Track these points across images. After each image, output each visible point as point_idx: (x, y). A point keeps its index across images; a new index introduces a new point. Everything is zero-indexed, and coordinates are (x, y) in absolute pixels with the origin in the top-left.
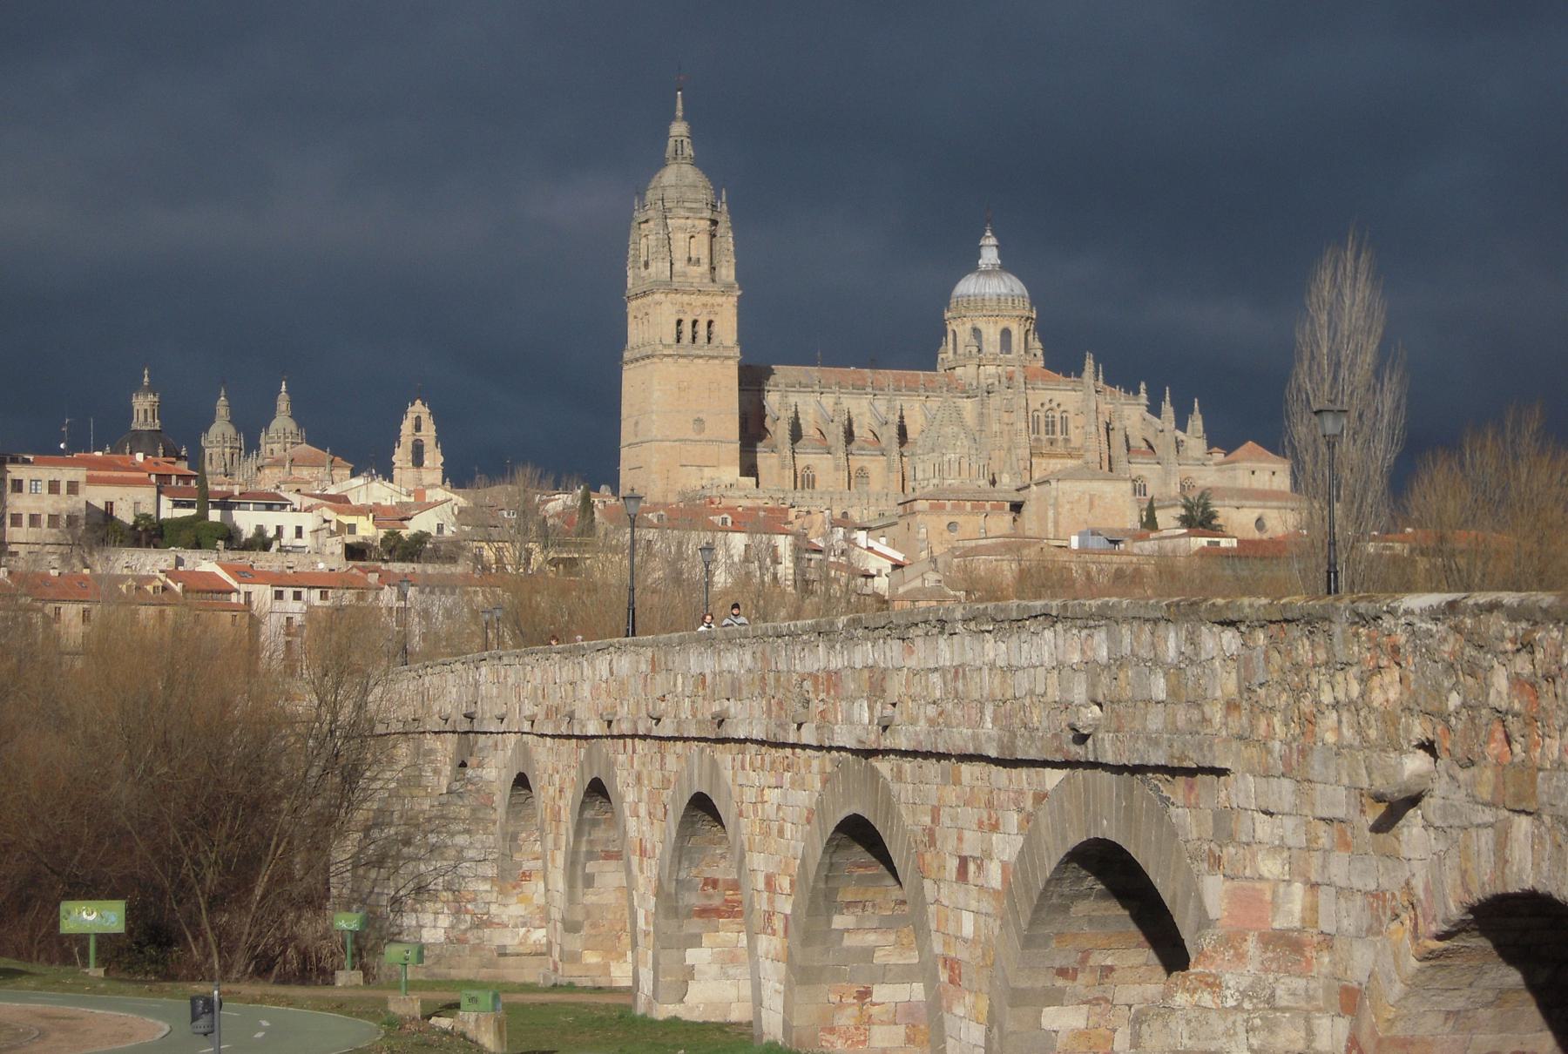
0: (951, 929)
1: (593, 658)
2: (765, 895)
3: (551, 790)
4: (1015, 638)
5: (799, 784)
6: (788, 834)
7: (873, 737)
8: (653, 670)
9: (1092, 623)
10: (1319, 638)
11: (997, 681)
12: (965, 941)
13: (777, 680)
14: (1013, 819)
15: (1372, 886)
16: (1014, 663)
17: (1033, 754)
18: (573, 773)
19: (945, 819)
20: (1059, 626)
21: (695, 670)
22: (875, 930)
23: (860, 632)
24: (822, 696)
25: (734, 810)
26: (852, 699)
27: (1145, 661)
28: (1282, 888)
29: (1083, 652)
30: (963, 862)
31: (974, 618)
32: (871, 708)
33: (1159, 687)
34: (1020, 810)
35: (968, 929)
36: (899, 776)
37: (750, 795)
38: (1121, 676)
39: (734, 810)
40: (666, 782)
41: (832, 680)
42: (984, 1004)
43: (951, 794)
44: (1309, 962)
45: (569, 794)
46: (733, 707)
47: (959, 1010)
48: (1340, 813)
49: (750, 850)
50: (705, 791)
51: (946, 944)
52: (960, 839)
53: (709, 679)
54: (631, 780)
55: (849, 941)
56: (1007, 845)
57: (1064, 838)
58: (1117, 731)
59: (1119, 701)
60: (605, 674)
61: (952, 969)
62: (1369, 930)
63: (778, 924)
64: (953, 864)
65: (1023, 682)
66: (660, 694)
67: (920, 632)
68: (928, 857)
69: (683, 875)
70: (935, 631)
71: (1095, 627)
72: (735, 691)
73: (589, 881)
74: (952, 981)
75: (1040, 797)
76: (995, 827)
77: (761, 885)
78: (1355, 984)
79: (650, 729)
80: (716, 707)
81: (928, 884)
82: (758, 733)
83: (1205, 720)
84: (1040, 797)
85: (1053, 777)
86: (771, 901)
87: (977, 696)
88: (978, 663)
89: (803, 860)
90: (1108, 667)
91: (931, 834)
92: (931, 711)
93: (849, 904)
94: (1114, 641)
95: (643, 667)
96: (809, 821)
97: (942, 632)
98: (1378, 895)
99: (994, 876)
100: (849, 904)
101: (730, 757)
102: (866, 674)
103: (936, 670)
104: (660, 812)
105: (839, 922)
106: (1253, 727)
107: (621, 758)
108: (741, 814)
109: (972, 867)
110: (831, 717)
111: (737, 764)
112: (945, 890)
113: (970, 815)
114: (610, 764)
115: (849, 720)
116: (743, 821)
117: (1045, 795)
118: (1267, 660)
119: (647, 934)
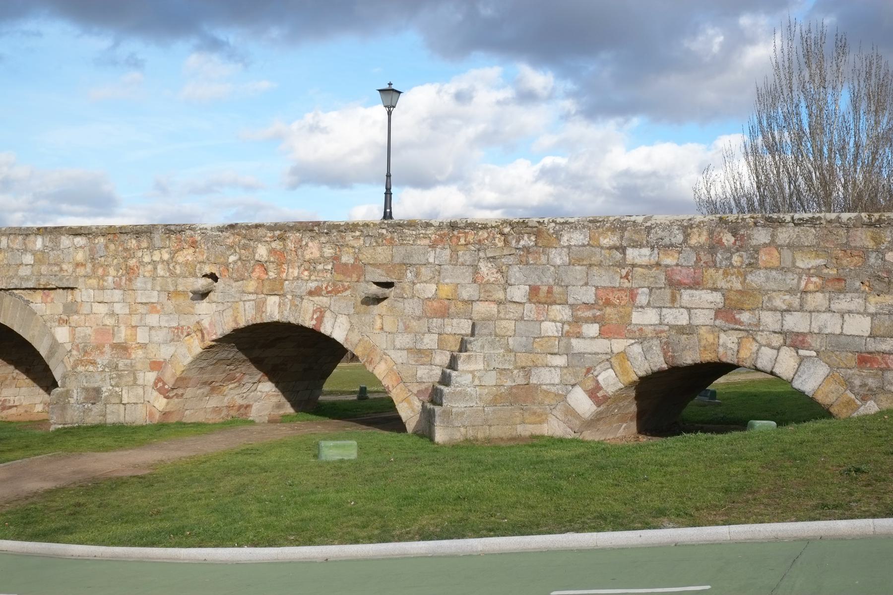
15: (175, 325)
27: (18, 250)
28: (116, 329)
33: (28, 259)
44: (130, 354)
62: (172, 340)
78: (162, 360)
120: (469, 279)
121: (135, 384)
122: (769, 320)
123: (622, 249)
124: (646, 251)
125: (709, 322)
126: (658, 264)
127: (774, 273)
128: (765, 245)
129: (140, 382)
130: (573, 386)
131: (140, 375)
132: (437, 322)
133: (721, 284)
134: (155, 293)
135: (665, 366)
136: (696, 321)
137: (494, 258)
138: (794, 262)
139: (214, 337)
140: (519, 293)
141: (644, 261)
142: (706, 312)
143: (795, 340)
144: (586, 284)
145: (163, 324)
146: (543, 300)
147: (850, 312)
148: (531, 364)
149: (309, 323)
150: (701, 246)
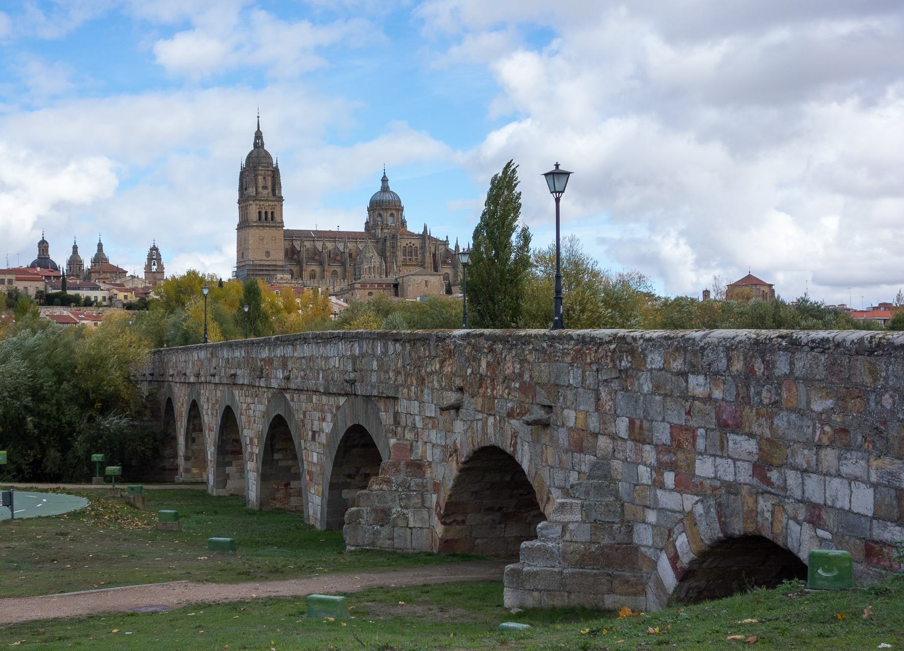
0: (310, 459)
1: (192, 352)
3: (179, 404)
4: (328, 347)
5: (260, 403)
6: (256, 422)
7: (283, 384)
8: (212, 357)
9: (353, 340)
11: (323, 363)
12: (315, 464)
13: (253, 361)
14: (329, 417)
16: (329, 355)
17: (335, 391)
18: (186, 397)
19: (307, 416)
21: (226, 356)
22: (291, 459)
23: (279, 343)
24: (267, 367)
25: (239, 412)
26: (277, 369)
29: (351, 351)
30: (314, 433)
31: (316, 337)
32: (283, 373)
34: (332, 413)
35: (315, 460)
36: (293, 400)
37: (244, 406)
38: (363, 360)
39: (239, 412)
40: (217, 401)
41: (269, 361)
42: (320, 489)
43: (310, 406)
45: (185, 405)
46: (239, 372)
51: (308, 465)
52: (312, 424)
53: (230, 361)
54: (205, 400)
55: (281, 464)
56: (327, 427)
57: (346, 423)
58: (362, 382)
59: (362, 370)
60: (196, 358)
61: (310, 476)
64: (310, 433)
66: (214, 366)
67: (298, 343)
69: (224, 438)
70: (303, 342)
71: (354, 341)
72: (239, 366)
75: (338, 408)
76: (324, 420)
77: (248, 442)
79: (211, 380)
80: (233, 372)
81: (302, 441)
82: (246, 382)
84: (338, 408)
85: (342, 400)
86: (252, 448)
87: (317, 368)
88: (317, 355)
89: (262, 431)
90: (359, 357)
91: (303, 421)
93: (280, 450)
94: (361, 347)
95: (209, 356)
96: (264, 417)
97: (305, 343)
99: (323, 439)
100: (280, 450)
102: (281, 360)
103: (304, 357)
105: (277, 456)
107: (202, 391)
108: (241, 414)
109: (317, 436)
110: (270, 376)
111: (240, 394)
112: (308, 444)
113: (317, 415)
114: (199, 394)
115: (276, 378)
117: (340, 407)
119: (211, 462)
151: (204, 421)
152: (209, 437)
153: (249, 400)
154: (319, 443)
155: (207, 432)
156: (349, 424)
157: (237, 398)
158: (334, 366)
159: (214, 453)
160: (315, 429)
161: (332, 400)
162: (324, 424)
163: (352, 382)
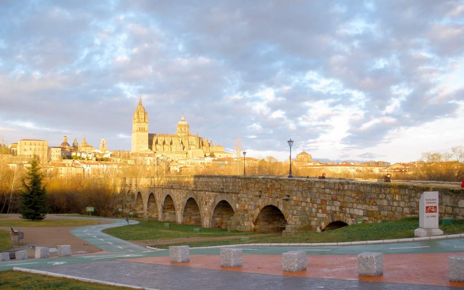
2: (178, 206)
4: (213, 179)
10: (250, 180)
16: (213, 181)
17: (216, 191)
20: (219, 178)
21: (168, 180)
25: (173, 197)
32: (194, 185)
33: (231, 184)
34: (213, 197)
36: (197, 193)
37: (176, 195)
42: (209, 218)
44: (248, 212)
45: (147, 194)
47: (205, 219)
48: (252, 198)
49: (176, 201)
50: (169, 194)
56: (212, 201)
63: (180, 210)
64: (205, 203)
65: (214, 183)
68: (201, 202)
73: (150, 205)
74: (205, 215)
76: (210, 199)
83: (236, 188)
85: (218, 193)
89: (184, 202)
92: (202, 186)
97: (204, 177)
98: (256, 205)
99: (210, 204)
101: (173, 191)
104: (162, 197)
105: (188, 209)
106: (242, 189)
108: (174, 197)
109: (207, 203)
114: (154, 191)
116: (175, 198)
118: (244, 182)
120: (301, 196)
121: (248, 220)
122: (348, 210)
123: (324, 189)
124: (328, 190)
125: (338, 210)
126: (330, 194)
127: (348, 197)
128: (347, 190)
129: (249, 220)
130: (318, 226)
131: (250, 218)
132: (296, 207)
133: (340, 200)
134: (252, 196)
135: (332, 222)
136: (337, 210)
137: (305, 190)
138: (351, 195)
139: (261, 208)
140: (309, 200)
141: (328, 192)
142: (338, 207)
143: (352, 216)
144: (319, 198)
145: (253, 204)
146: (313, 202)
147: (360, 209)
148: (310, 220)
149: (276, 206)
150: (337, 189)
151: (156, 199)
152: (159, 204)
153: (178, 193)
154: (209, 205)
155: (158, 203)
156: (221, 200)
157: (173, 192)
158: (215, 184)
159: (161, 209)
160: (207, 201)
161: (213, 193)
162: (211, 200)
163: (222, 189)
